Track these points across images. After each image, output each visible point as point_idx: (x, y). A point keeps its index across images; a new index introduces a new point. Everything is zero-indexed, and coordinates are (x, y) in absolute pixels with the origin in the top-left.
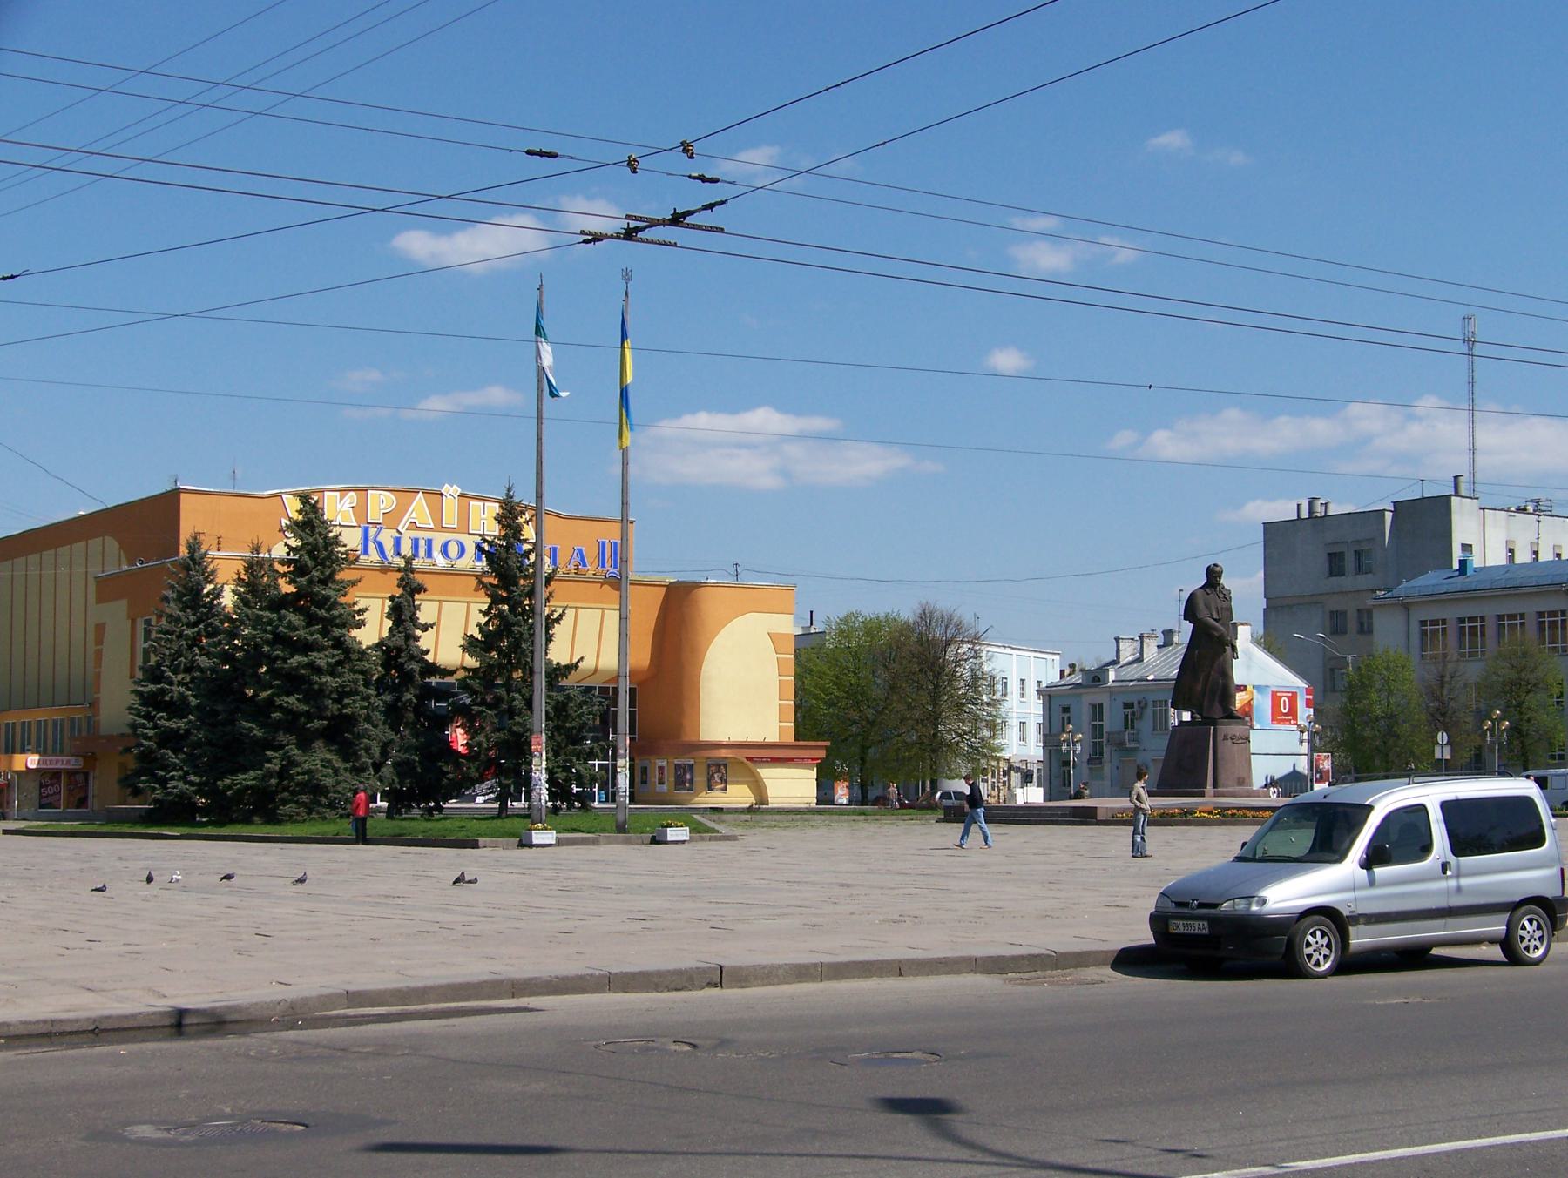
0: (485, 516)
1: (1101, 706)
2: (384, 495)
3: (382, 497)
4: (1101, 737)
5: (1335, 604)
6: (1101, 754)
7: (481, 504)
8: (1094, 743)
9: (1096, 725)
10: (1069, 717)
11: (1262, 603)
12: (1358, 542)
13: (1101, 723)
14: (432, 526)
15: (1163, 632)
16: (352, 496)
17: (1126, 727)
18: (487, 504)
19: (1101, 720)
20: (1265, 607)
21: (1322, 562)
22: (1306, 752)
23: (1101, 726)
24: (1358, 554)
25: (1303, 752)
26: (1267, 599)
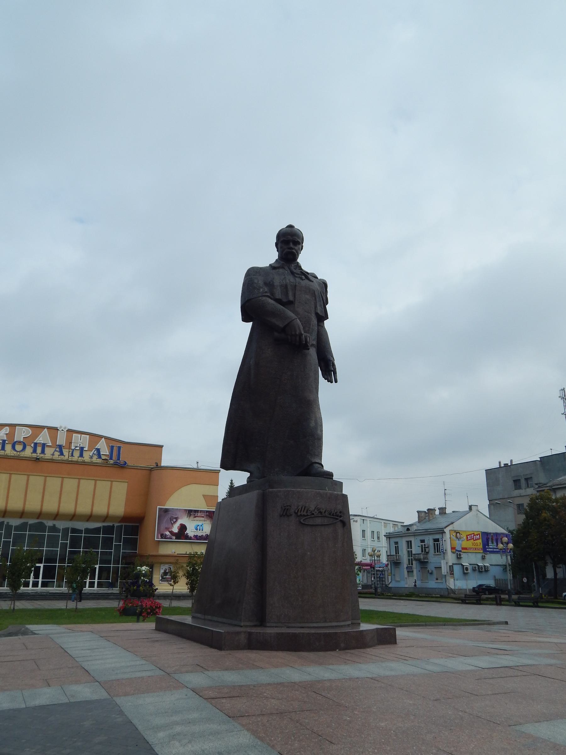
0: (81, 441)
1: (411, 541)
2: (24, 429)
3: (24, 430)
4: (412, 557)
5: (518, 501)
6: (412, 564)
7: (79, 435)
8: (409, 559)
9: (409, 551)
10: (398, 546)
11: (488, 502)
13: (411, 550)
14: (50, 445)
16: (7, 428)
17: (422, 551)
18: (82, 435)
19: (411, 548)
20: (489, 504)
21: (511, 483)
22: (93, 482)
23: (411, 551)
24: (527, 480)
25: (76, 484)
26: (489, 500)
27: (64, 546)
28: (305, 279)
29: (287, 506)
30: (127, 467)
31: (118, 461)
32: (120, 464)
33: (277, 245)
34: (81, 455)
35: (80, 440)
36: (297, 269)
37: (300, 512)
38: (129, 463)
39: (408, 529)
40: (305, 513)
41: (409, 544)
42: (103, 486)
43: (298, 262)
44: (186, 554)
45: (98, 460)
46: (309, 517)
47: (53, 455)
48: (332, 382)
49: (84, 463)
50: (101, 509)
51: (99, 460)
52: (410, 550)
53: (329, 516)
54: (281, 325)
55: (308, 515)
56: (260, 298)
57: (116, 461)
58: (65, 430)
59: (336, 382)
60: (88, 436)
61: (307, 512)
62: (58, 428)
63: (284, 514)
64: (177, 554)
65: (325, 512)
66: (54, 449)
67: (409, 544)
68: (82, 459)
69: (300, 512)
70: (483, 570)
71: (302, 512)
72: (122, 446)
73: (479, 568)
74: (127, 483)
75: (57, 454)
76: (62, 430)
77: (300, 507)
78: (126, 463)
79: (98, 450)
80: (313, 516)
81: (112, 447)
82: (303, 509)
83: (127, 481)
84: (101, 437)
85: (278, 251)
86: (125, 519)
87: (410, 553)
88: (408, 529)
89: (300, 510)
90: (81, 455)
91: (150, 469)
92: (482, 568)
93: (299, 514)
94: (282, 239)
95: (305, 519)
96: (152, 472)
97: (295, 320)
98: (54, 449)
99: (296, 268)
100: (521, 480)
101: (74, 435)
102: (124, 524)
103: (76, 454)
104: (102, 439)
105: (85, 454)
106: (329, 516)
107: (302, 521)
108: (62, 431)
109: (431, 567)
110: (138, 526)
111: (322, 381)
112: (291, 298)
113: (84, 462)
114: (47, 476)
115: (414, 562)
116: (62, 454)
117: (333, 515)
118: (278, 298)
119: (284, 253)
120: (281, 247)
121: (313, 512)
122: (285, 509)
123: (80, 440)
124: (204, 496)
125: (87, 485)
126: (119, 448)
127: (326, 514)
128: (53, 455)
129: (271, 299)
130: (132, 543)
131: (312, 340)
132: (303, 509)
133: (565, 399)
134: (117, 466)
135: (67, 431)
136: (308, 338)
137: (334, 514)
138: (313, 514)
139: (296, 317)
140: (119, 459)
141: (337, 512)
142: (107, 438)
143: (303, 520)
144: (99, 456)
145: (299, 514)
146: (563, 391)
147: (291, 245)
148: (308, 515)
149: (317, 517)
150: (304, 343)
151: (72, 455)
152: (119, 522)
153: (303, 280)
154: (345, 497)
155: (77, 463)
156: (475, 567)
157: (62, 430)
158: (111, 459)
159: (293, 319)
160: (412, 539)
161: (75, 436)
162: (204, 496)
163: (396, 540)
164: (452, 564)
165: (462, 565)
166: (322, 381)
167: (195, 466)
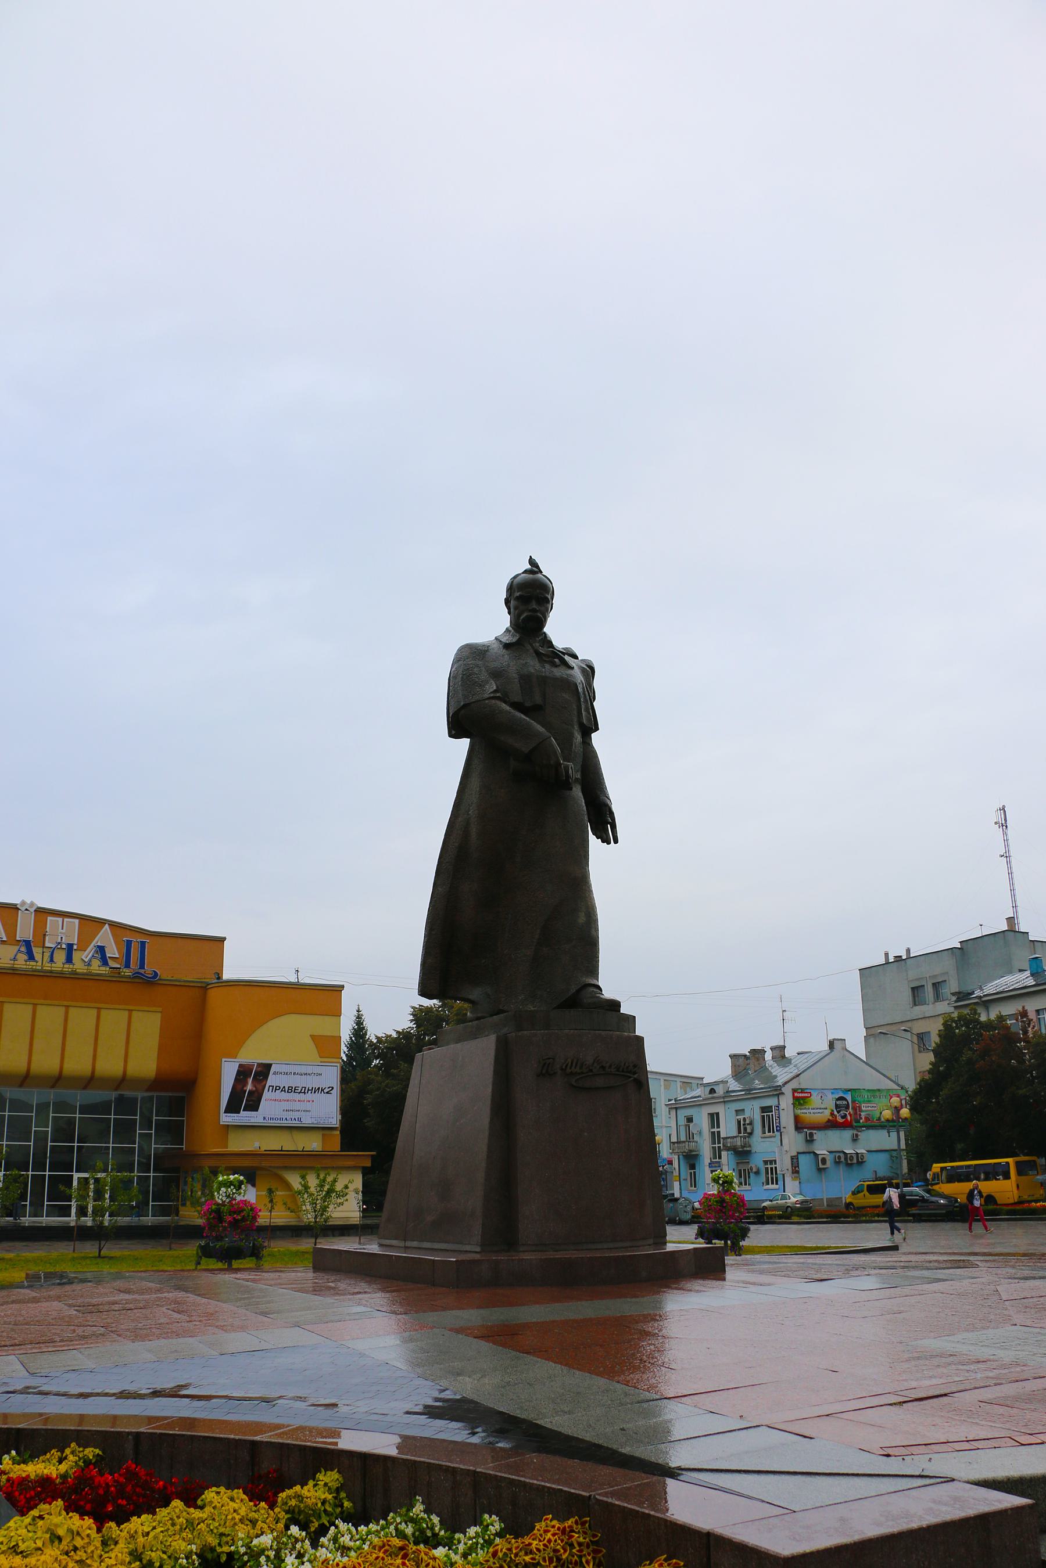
0: (64, 931)
1: (718, 1114)
4: (719, 1143)
5: (919, 1027)
6: (720, 1157)
7: (60, 920)
8: (714, 1148)
12: (935, 976)
13: (718, 1130)
15: (771, 1049)
17: (740, 1132)
19: (718, 1127)
20: (865, 1035)
21: (908, 994)
23: (719, 1132)
24: (935, 985)
27: (41, 1138)
28: (559, 666)
29: (549, 1059)
30: (161, 982)
31: (142, 971)
32: (146, 977)
33: (507, 602)
34: (69, 960)
35: (62, 929)
36: (545, 645)
37: (571, 1068)
38: (164, 974)
39: (712, 1091)
40: (578, 1070)
41: (714, 1118)
42: (114, 1019)
43: (545, 633)
44: (282, 1151)
45: (101, 968)
46: (584, 1075)
47: (15, 959)
48: (609, 843)
49: (75, 976)
50: (110, 1065)
51: (104, 968)
52: (716, 1130)
53: (617, 1073)
54: (526, 749)
55: (582, 1073)
56: (487, 701)
57: (137, 971)
58: (32, 910)
59: (616, 841)
60: (77, 921)
61: (581, 1068)
62: (18, 906)
63: (544, 1071)
64: (265, 1151)
65: (610, 1066)
66: (17, 948)
67: (714, 1118)
68: (71, 966)
69: (571, 1068)
70: (855, 1161)
71: (573, 1068)
72: (148, 941)
73: (846, 1159)
74: (159, 1015)
75: (22, 958)
76: (26, 910)
77: (570, 1061)
78: (156, 974)
79: (101, 950)
80: (591, 1074)
81: (129, 943)
82: (574, 1065)
83: (160, 1009)
84: (101, 922)
85: (509, 613)
86: (158, 1083)
87: (715, 1137)
88: (712, 1091)
89: (570, 1063)
90: (69, 960)
91: (204, 985)
92: (852, 1158)
93: (568, 1070)
94: (517, 594)
95: (578, 1079)
96: (209, 991)
97: (548, 740)
98: (17, 948)
99: (543, 645)
100: (926, 986)
101: (49, 918)
102: (155, 1094)
103: (60, 957)
104: (104, 929)
105: (76, 956)
106: (617, 1073)
107: (574, 1084)
108: (26, 911)
109: (757, 1161)
110: (184, 1097)
111: (593, 841)
112: (538, 699)
113: (74, 973)
114: (37, 1004)
115: (724, 1154)
116: (31, 957)
117: (623, 1071)
118: (516, 700)
119: (522, 618)
120: (516, 608)
121: (591, 1068)
122: (545, 1064)
123: (62, 929)
124: (313, 1037)
125: (83, 1018)
126: (143, 944)
127: (612, 1070)
128: (15, 959)
129: (505, 702)
130: (174, 1131)
131: (573, 770)
132: (574, 1065)
133: (1006, 827)
134: (141, 981)
135: (35, 911)
136: (570, 770)
137: (625, 1070)
138: (591, 1071)
139: (548, 734)
140: (142, 966)
141: (629, 1066)
142: (115, 926)
143: (576, 1081)
144: (104, 961)
145: (568, 1070)
146: (1002, 811)
147: (534, 605)
148: (582, 1073)
149: (599, 1074)
150: (564, 778)
151: (52, 960)
152: (149, 1090)
153: (556, 666)
154: (640, 1040)
155: (60, 976)
156: (839, 1157)
157: (26, 910)
158: (127, 966)
159: (546, 737)
160: (719, 1109)
161: (51, 920)
162: (313, 1037)
163: (689, 1112)
164: (795, 1154)
165: (814, 1153)
166: (593, 841)
167: (293, 979)
